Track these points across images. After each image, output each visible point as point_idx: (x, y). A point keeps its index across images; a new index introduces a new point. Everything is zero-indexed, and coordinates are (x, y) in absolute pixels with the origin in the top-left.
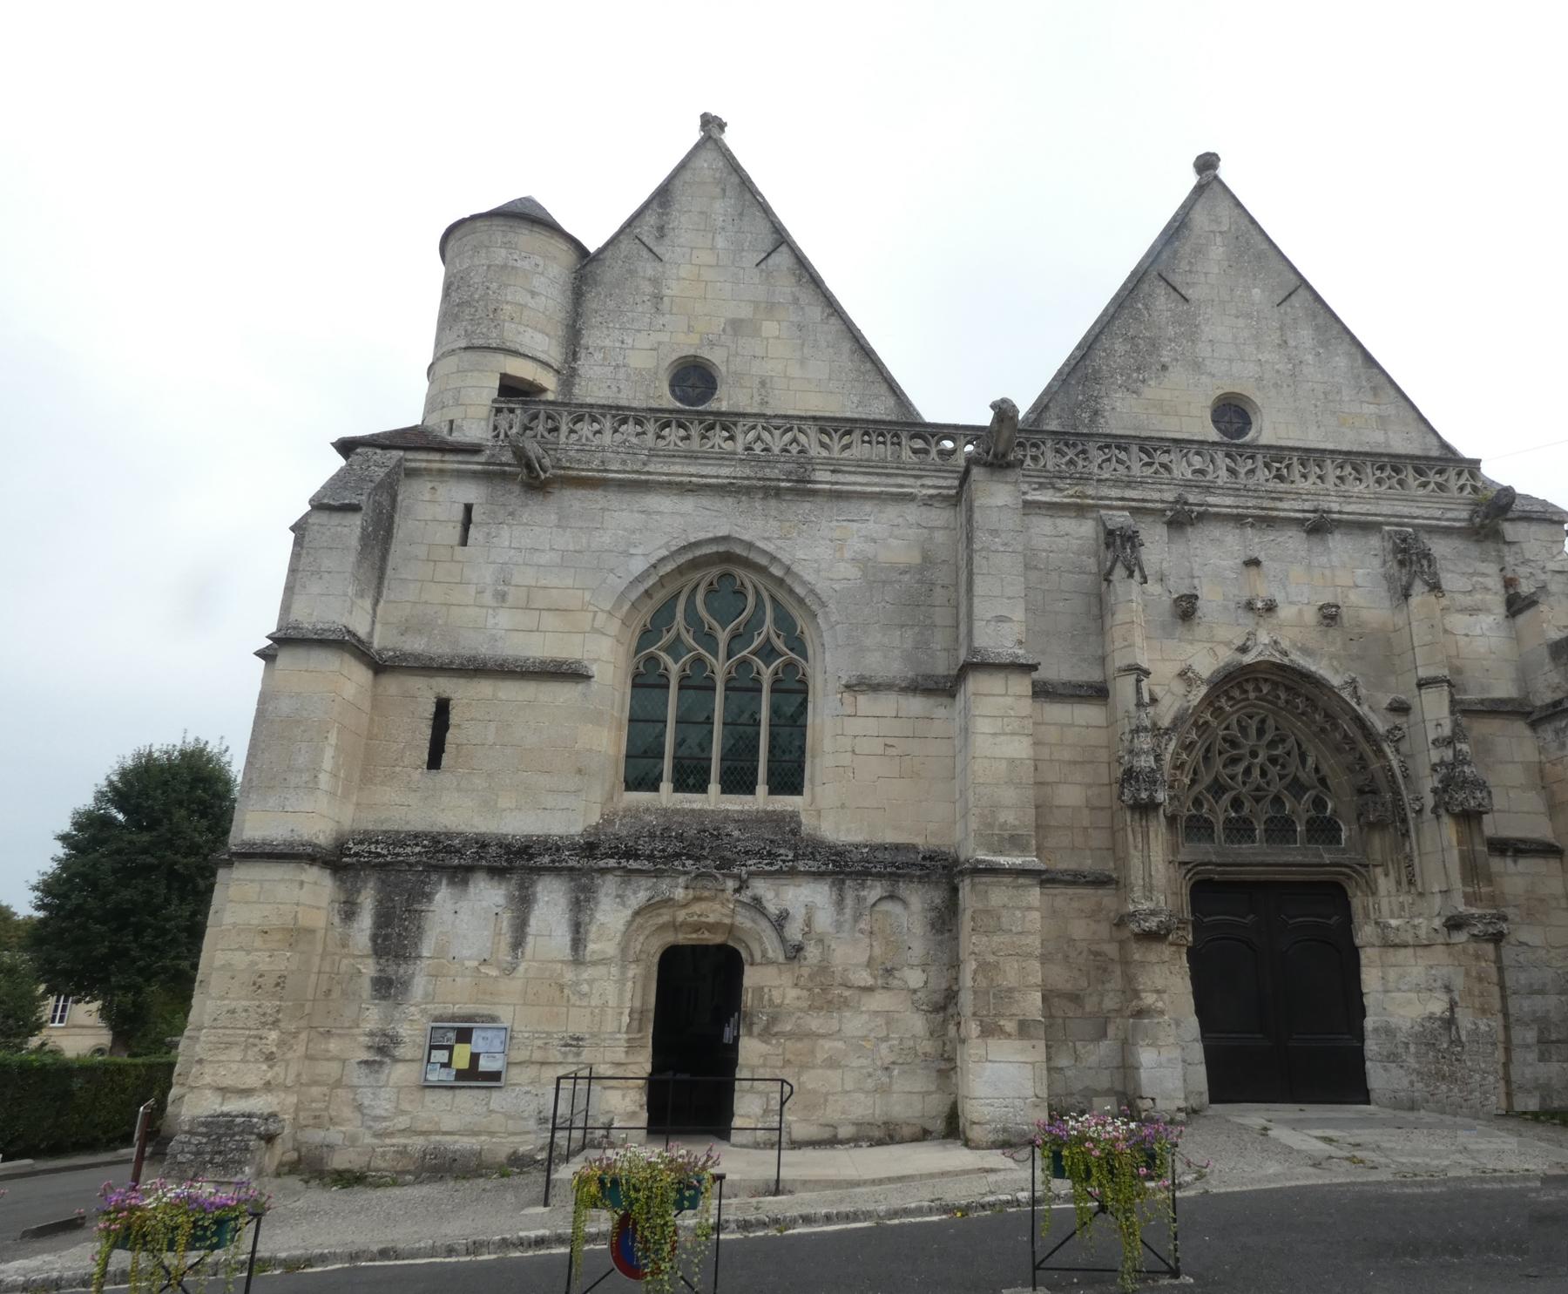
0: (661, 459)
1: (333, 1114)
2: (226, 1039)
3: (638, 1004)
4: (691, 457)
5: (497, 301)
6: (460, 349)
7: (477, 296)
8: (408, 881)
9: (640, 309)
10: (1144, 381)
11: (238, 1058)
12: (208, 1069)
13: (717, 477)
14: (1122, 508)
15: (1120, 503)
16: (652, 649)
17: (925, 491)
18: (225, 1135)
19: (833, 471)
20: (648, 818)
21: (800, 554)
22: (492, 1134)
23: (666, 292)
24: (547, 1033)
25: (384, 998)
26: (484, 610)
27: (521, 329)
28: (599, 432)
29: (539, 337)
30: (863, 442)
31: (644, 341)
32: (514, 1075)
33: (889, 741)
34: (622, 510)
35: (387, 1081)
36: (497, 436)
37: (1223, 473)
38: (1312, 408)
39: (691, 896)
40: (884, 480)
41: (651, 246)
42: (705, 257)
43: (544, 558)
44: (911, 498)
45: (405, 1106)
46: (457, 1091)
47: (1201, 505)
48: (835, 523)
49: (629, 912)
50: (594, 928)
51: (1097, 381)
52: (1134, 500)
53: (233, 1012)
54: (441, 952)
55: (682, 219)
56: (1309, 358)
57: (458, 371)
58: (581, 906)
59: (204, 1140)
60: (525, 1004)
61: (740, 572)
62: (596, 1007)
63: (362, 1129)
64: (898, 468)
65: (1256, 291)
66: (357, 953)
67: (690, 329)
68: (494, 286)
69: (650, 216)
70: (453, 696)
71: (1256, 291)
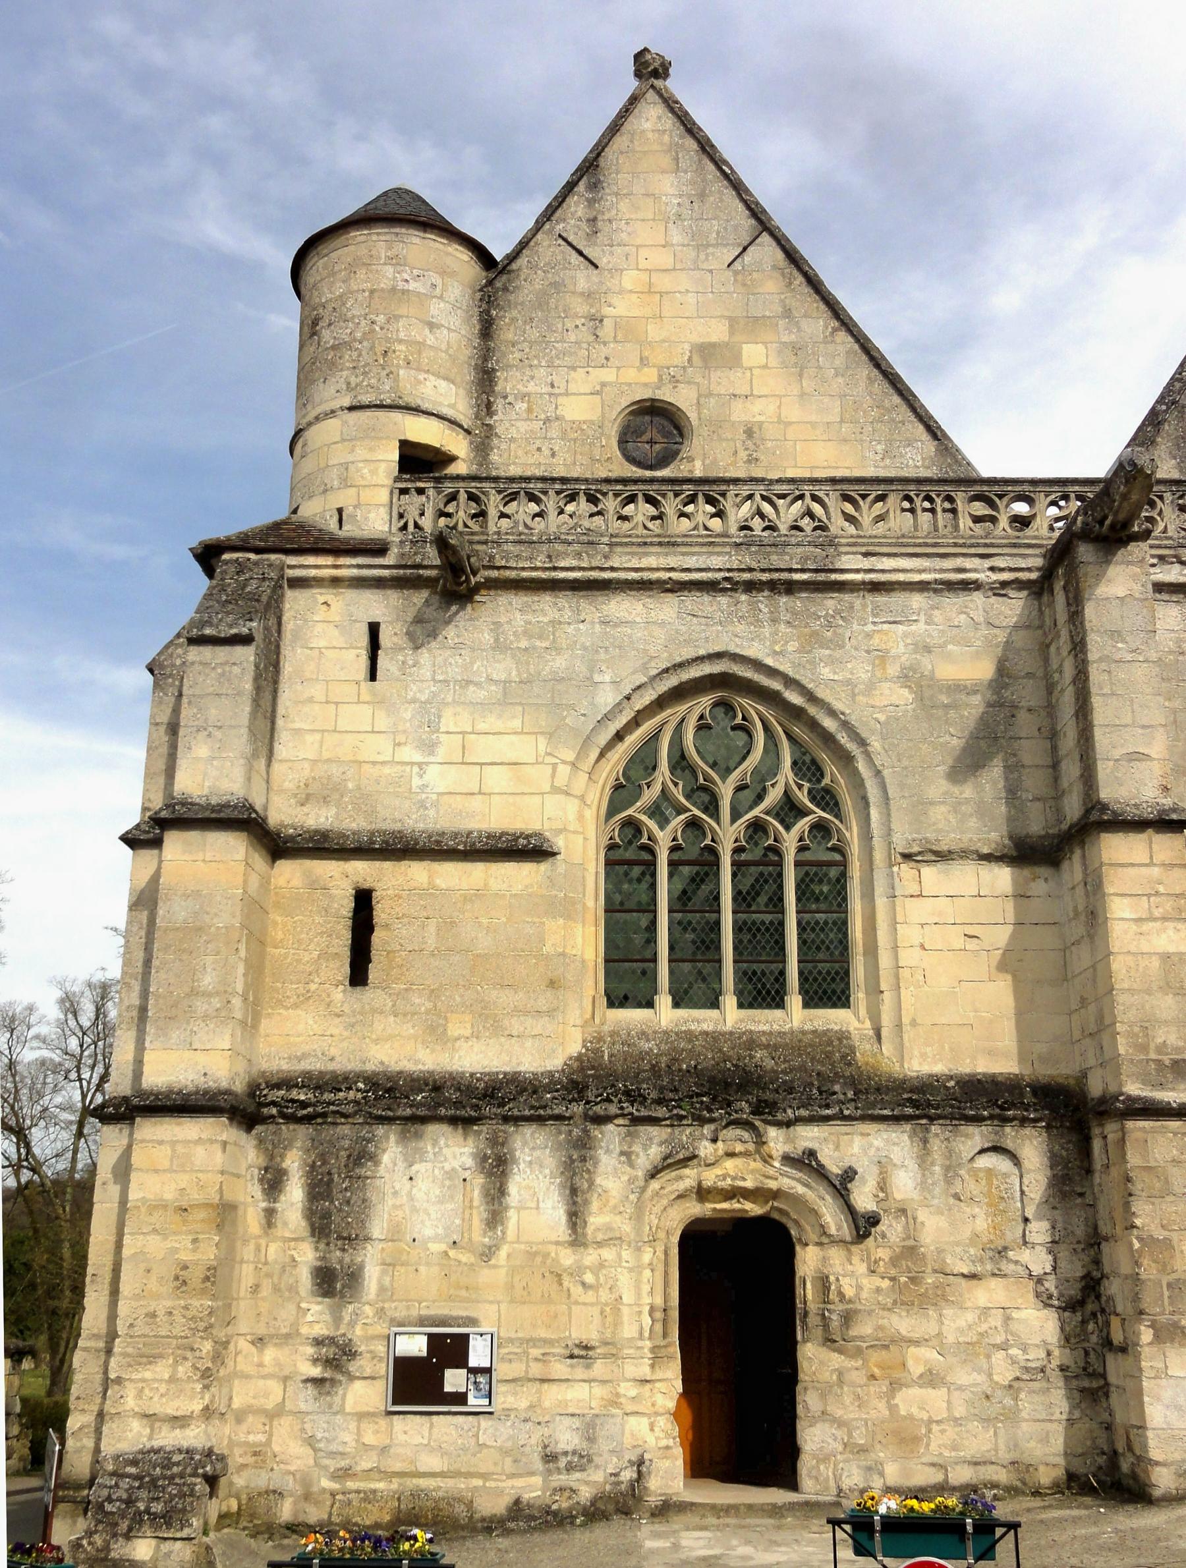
0: (628, 550)
2: (146, 1351)
3: (659, 1301)
5: (388, 340)
6: (342, 409)
7: (359, 335)
9: (573, 338)
11: (166, 1376)
16: (629, 812)
17: (995, 577)
19: (866, 555)
20: (646, 1046)
21: (826, 672)
23: (607, 311)
26: (408, 768)
27: (421, 377)
28: (540, 514)
29: (443, 384)
30: (903, 510)
31: (581, 381)
33: (970, 930)
35: (343, 1405)
36: (404, 527)
39: (721, 1152)
44: (976, 586)
48: (870, 627)
53: (153, 1315)
54: (396, 1233)
57: (343, 440)
60: (512, 1301)
61: (747, 704)
62: (606, 1304)
64: (956, 545)
66: (287, 1235)
67: (644, 362)
68: (381, 319)
69: (577, 204)
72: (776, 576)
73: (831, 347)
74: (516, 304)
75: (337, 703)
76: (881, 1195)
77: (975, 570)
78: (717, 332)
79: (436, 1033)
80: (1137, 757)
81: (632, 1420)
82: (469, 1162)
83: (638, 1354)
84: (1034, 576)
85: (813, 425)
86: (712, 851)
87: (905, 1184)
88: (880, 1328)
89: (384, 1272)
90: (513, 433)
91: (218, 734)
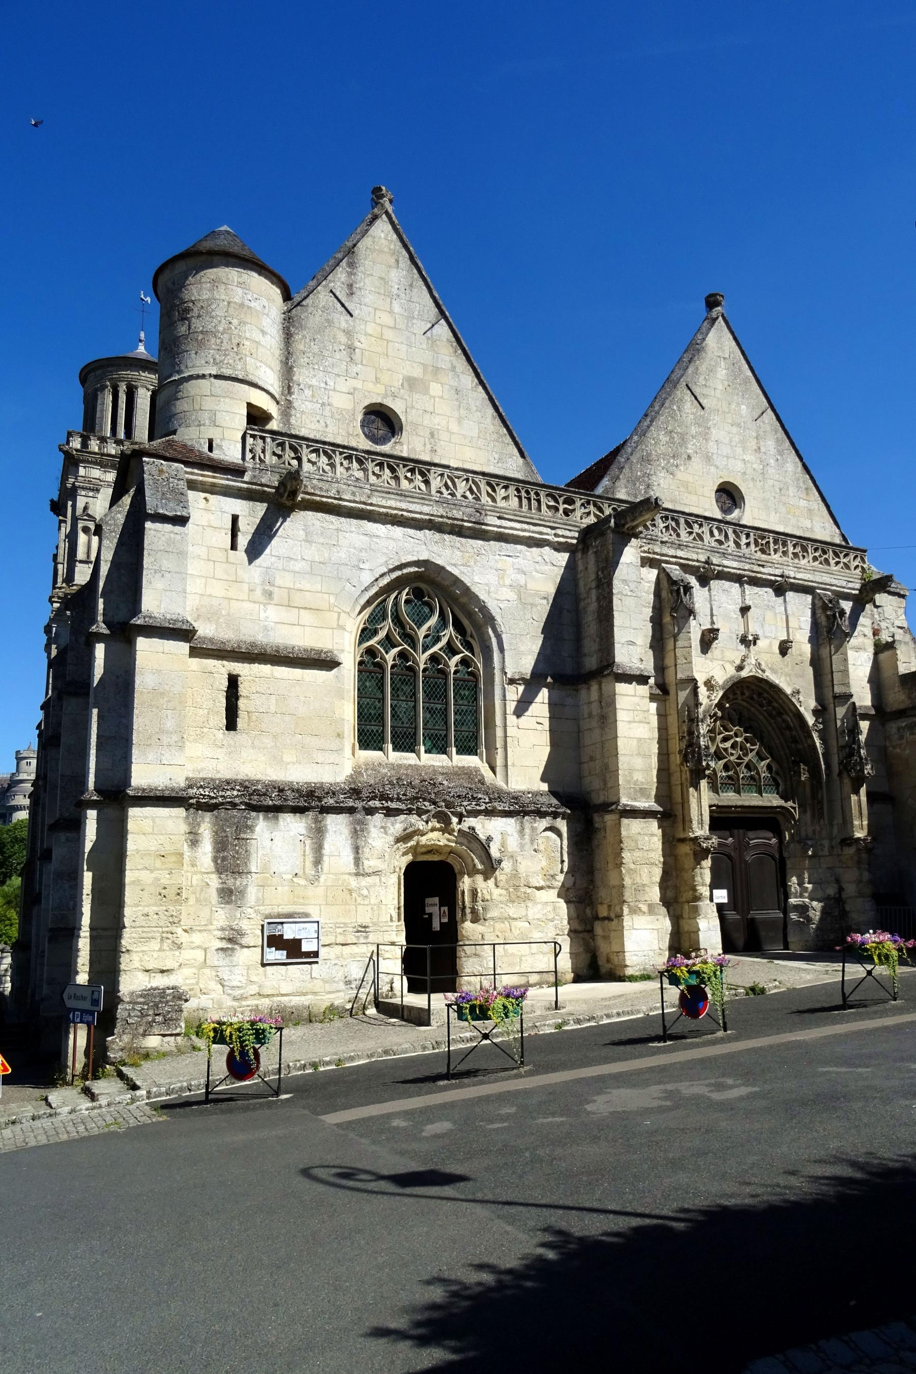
0: (381, 494)
1: (202, 986)
2: (144, 935)
4: (401, 495)
5: (240, 336)
6: (210, 375)
7: (221, 329)
8: (234, 817)
9: (338, 357)
10: (677, 466)
11: (157, 949)
12: (135, 957)
13: (421, 513)
14: (675, 564)
15: (674, 560)
18: (161, 1002)
19: (499, 518)
21: (477, 579)
22: (315, 993)
23: (357, 344)
24: (344, 923)
25: (228, 903)
27: (259, 364)
31: (343, 385)
32: (323, 952)
33: (539, 720)
34: (351, 532)
37: (731, 543)
38: (772, 499)
39: (430, 828)
40: (532, 528)
41: (343, 301)
42: (386, 319)
43: (299, 566)
45: (254, 978)
46: (289, 967)
47: (719, 566)
48: (497, 557)
49: (391, 839)
50: (366, 850)
51: (649, 461)
52: (681, 558)
54: (265, 869)
55: (366, 280)
56: (772, 461)
58: (357, 833)
59: (146, 1007)
63: (225, 996)
65: (743, 407)
70: (241, 673)
71: (743, 407)
72: (455, 522)
73: (475, 394)
74: (305, 328)
75: (214, 561)
77: (547, 534)
78: (417, 372)
79: (277, 760)
80: (632, 643)
82: (304, 832)
83: (390, 929)
84: (575, 541)
85: (464, 436)
86: (411, 669)
87: (513, 843)
89: (258, 891)
90: (303, 408)
91: (167, 575)
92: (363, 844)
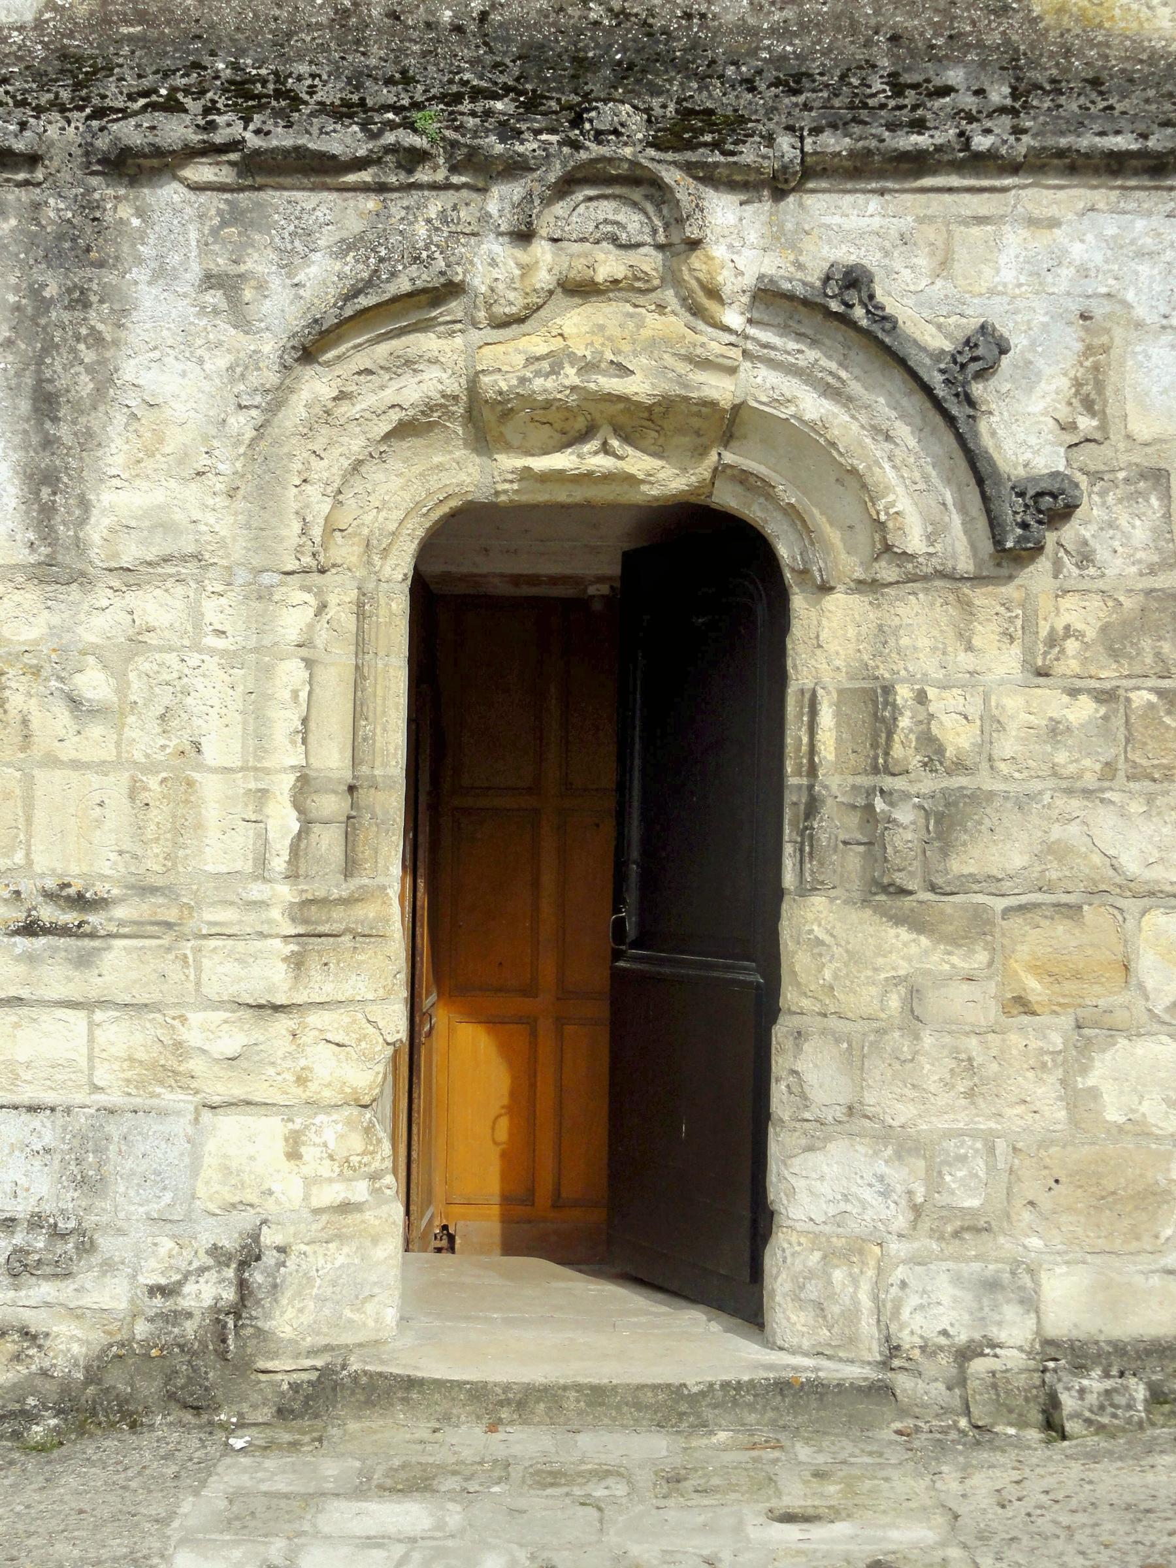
39: (543, 278)
62: (151, 768)
76: (1086, 423)
81: (228, 1125)
83: (251, 922)
88: (1054, 851)
92: (86, 386)
